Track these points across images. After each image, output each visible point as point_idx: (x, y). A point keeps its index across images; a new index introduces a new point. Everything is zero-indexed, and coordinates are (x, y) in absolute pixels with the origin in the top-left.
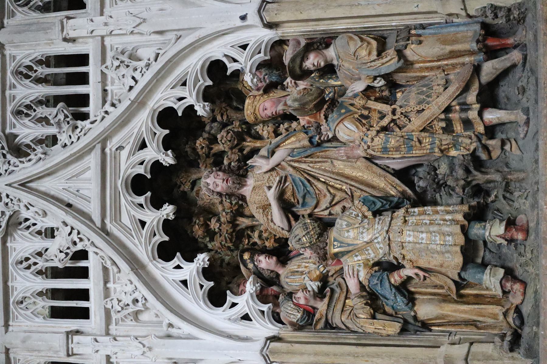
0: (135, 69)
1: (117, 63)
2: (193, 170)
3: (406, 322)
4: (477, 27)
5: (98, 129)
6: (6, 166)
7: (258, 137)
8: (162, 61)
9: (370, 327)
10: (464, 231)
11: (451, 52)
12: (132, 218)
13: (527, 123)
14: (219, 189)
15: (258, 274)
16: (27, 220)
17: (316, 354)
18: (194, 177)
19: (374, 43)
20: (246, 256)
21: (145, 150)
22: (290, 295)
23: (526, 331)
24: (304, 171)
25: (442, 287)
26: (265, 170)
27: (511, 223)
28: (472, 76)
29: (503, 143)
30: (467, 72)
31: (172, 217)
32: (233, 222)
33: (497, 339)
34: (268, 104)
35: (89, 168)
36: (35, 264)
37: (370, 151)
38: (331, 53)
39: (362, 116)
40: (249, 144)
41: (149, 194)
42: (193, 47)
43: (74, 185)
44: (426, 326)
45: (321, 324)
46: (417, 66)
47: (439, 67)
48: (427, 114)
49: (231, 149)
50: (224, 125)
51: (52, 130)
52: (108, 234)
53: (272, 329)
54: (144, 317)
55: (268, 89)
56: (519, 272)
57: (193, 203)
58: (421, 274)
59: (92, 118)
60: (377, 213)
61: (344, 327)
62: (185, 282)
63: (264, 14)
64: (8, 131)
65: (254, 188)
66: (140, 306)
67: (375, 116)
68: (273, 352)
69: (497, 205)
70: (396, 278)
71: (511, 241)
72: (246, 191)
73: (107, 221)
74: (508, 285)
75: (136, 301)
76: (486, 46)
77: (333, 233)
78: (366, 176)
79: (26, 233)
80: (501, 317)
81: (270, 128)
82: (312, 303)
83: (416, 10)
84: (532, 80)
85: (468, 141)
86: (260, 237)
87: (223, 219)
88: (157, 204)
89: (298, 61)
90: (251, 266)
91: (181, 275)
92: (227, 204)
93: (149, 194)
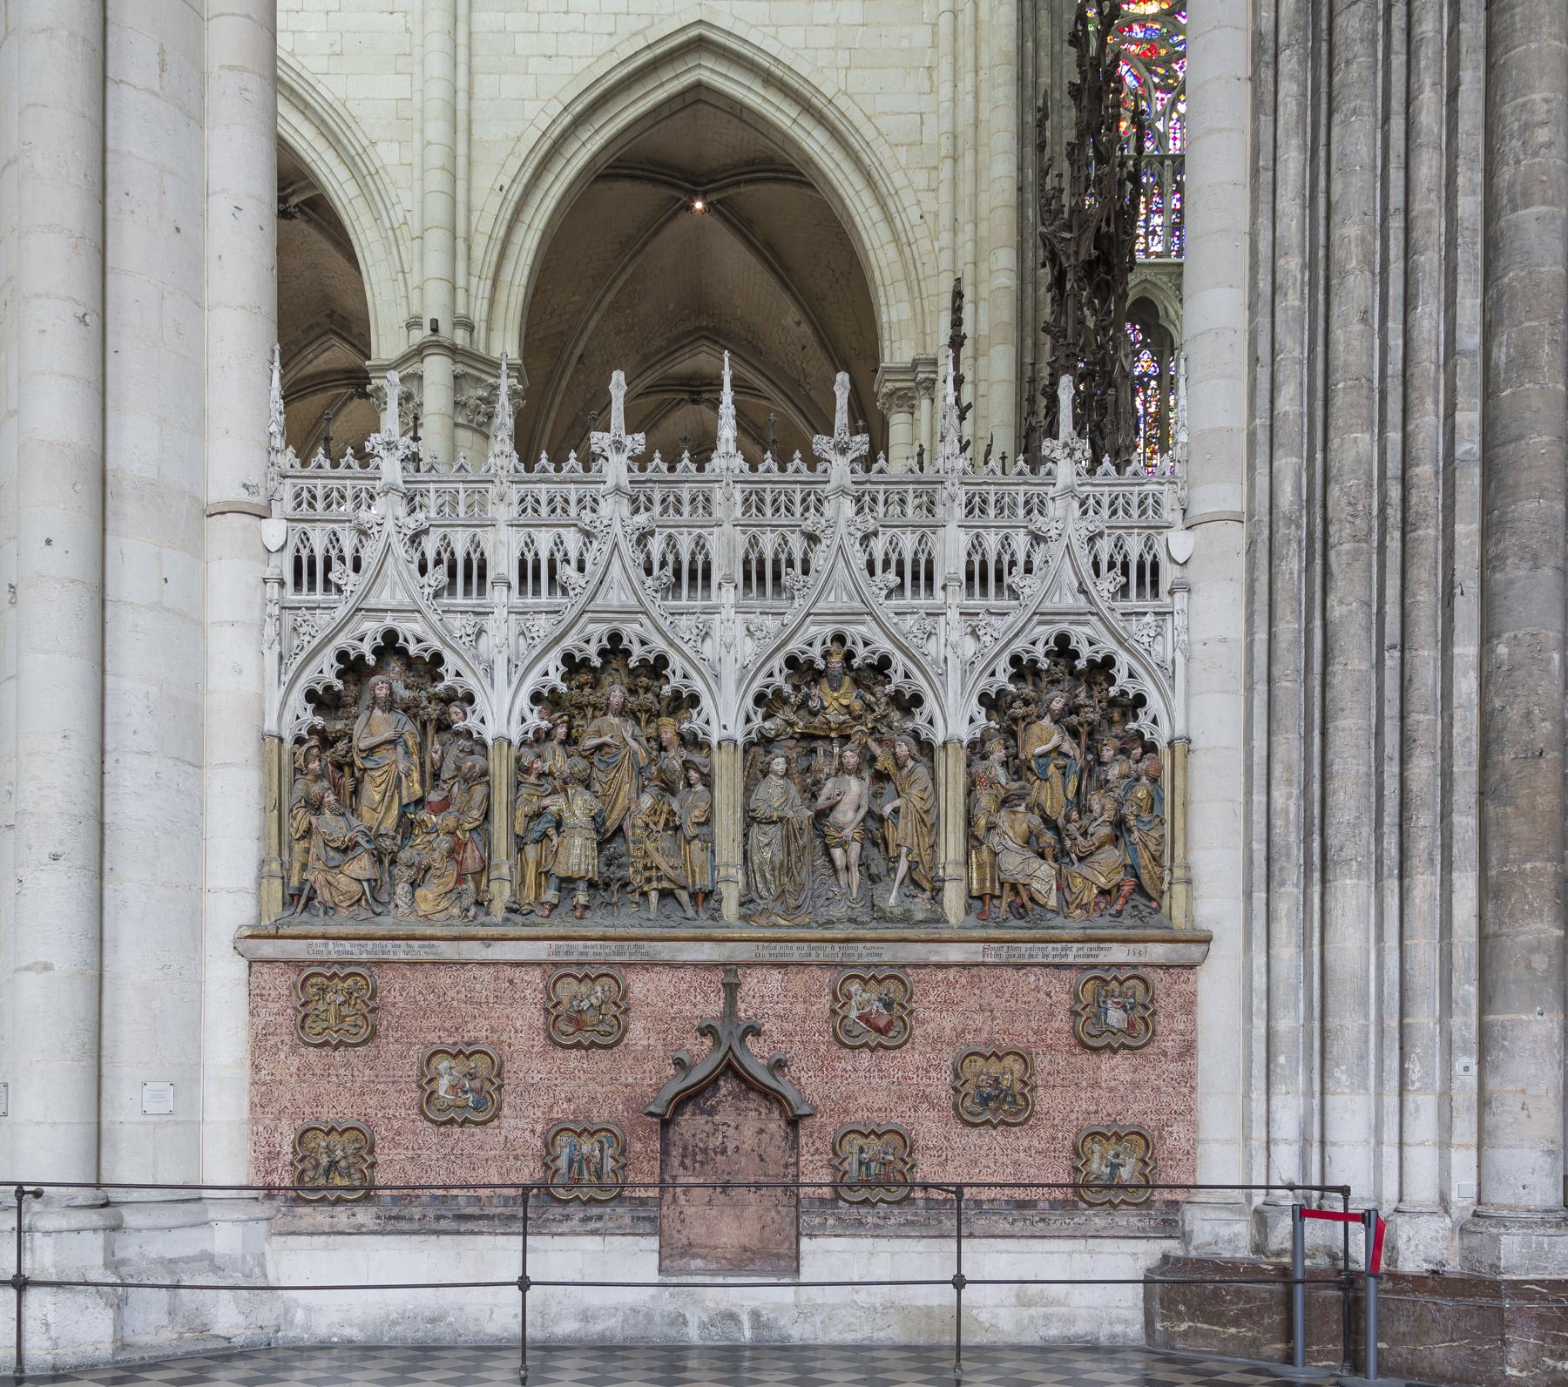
8: (700, 664)
9: (519, 813)
10: (582, 878)
23: (517, 918)
27: (586, 907)
30: (683, 883)
38: (700, 787)
43: (615, 586)
44: (521, 850)
48: (656, 855)
53: (516, 741)
55: (680, 736)
56: (555, 912)
60: (593, 818)
70: (551, 832)
77: (580, 789)
78: (618, 806)
88: (602, 653)
91: (552, 671)
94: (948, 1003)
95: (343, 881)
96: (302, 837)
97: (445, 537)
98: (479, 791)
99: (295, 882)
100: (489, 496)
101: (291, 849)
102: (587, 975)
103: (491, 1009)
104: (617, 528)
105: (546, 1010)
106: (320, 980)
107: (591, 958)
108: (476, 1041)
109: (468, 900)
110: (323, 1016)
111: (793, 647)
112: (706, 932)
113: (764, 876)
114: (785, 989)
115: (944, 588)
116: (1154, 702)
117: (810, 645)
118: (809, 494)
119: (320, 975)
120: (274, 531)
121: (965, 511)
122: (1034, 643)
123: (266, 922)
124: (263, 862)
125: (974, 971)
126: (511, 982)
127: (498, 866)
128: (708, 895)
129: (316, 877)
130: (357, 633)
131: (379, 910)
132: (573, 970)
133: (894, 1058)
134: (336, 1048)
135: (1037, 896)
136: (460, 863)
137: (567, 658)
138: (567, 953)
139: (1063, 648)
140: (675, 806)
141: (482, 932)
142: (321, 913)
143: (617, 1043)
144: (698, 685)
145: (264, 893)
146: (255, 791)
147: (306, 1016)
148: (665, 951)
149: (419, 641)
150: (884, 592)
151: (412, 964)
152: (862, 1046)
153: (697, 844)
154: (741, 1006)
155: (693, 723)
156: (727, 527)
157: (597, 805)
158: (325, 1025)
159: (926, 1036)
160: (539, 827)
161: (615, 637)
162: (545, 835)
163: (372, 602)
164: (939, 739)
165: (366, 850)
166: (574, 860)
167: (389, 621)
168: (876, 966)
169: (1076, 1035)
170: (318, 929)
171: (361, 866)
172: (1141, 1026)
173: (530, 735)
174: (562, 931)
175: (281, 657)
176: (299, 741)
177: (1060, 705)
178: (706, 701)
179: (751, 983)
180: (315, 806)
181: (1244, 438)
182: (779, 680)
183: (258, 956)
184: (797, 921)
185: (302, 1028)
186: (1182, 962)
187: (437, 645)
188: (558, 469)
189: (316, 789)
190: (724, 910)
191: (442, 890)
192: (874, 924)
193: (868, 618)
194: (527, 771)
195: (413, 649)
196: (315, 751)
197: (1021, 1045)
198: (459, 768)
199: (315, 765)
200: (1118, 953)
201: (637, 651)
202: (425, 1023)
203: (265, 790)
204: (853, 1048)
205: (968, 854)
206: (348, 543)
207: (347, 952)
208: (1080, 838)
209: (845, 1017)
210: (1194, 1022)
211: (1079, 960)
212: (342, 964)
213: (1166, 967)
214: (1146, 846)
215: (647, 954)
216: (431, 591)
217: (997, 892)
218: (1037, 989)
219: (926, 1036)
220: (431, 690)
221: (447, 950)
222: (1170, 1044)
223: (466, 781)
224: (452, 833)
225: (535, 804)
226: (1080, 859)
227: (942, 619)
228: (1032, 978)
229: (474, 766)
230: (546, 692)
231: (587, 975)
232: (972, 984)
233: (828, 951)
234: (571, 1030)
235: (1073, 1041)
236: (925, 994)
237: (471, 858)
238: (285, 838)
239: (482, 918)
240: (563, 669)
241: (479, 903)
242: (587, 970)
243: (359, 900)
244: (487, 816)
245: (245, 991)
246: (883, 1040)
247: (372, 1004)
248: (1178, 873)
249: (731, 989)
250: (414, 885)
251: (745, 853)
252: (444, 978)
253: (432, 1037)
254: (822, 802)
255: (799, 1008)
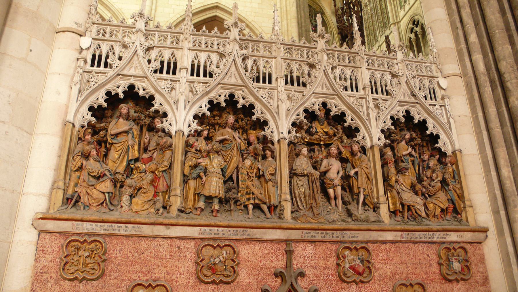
0: (267, 98)
1: (270, 93)
2: (233, 113)
3: (188, 176)
4: (277, 204)
5: (250, 85)
6: (240, 55)
7: (243, 134)
8: (270, 107)
9: (187, 165)
10: (216, 197)
11: (270, 196)
12: (222, 93)
13: (249, 218)
14: (229, 121)
15: (202, 131)
16: (222, 60)
17: (179, 147)
18: (231, 113)
19: (273, 172)
20: (208, 127)
21: (242, 99)
22: (197, 140)
24: (234, 147)
25: (198, 188)
26: (234, 136)
27: (218, 211)
28: (263, 202)
29: (242, 210)
30: (264, 200)
31: (221, 105)
32: (218, 124)
33: (182, 205)
34: (253, 138)
35: (237, 81)
36: (208, 61)
37: (241, 169)
39: (252, 167)
40: (241, 131)
41: (229, 99)
42: (274, 118)
45: (188, 150)
46: (266, 185)
47: (265, 191)
48: (252, 187)
49: (240, 125)
50: (246, 123)
51: (249, 70)
52: (217, 85)
53: (186, 134)
54: (191, 94)
55: (258, 138)
56: (203, 213)
57: (223, 112)
58: (203, 182)
59: (253, 84)
60: (222, 169)
61: (187, 157)
62: (201, 107)
63: (283, 139)
64: (250, 57)
65: (228, 131)
66: (195, 93)
67: (251, 171)
68: (179, 134)
69: (222, 207)
70: (202, 174)
71: (212, 211)
72: (228, 129)
73: (221, 85)
74: (199, 210)
75: (197, 92)
76: (271, 206)
77: (216, 155)
78: (231, 167)
79: (218, 59)
80: (189, 207)
81: (246, 138)
82: (195, 147)
83: (283, 185)
84: (261, 220)
85: (243, 199)
86: (213, 132)
87: (219, 121)
88: (225, 101)
89: (269, 149)
90: (205, 128)
91: (204, 106)
92: (223, 122)
93: (229, 99)
94: (388, 260)
95: (95, 193)
96: (77, 170)
97: (160, 51)
98: (168, 154)
99: (70, 192)
100: (181, 39)
101: (70, 177)
102: (218, 245)
103: (167, 262)
104: (235, 53)
105: (197, 264)
106: (76, 243)
107: (220, 236)
108: (159, 279)
109: (159, 205)
110: (76, 263)
111: (307, 105)
112: (275, 225)
113: (301, 200)
114: (315, 254)
115: (363, 89)
116: (443, 137)
117: (314, 105)
118: (309, 52)
119: (77, 240)
120: (86, 42)
121: (367, 64)
122: (398, 112)
123: (52, 211)
124: (54, 182)
125: (397, 245)
126: (179, 248)
127: (175, 189)
128: (276, 207)
129: (82, 190)
130: (117, 84)
131: (112, 208)
132: (211, 243)
133: (367, 287)
134: (81, 281)
135: (418, 211)
136: (156, 187)
137: (210, 102)
138: (209, 234)
139: (408, 116)
140: (260, 167)
141: (166, 221)
142: (82, 208)
143: (232, 281)
144: (268, 117)
145: (53, 197)
146: (57, 148)
147: (66, 263)
148: (258, 234)
149: (144, 90)
150: (342, 87)
151: (127, 236)
152: (352, 282)
153: (270, 184)
154: (295, 262)
155: (267, 132)
156: (279, 59)
157: (224, 164)
158: (76, 268)
159: (380, 276)
160: (196, 172)
161: (232, 96)
162: (199, 176)
163: (125, 72)
164: (368, 145)
165: (109, 178)
166: (213, 188)
167: (132, 81)
168: (356, 242)
169: (441, 274)
170: (78, 216)
171: (106, 186)
172: (466, 270)
173: (192, 132)
174: (207, 223)
175: (80, 91)
176: (83, 127)
177: (409, 137)
178: (271, 123)
179: (299, 250)
180: (86, 156)
181: (455, 52)
182: (302, 117)
183: (44, 229)
184: (319, 220)
185: (63, 269)
186: (477, 240)
187: (152, 91)
188: (210, 32)
189: (88, 148)
190: (285, 214)
191: (146, 199)
192: (353, 222)
193: (336, 97)
194: (192, 146)
195: (141, 93)
196: (90, 130)
197: (419, 281)
198: (158, 144)
199: (88, 137)
200: (453, 237)
201: (241, 102)
202: (132, 269)
203: (61, 148)
204: (348, 283)
205: (386, 194)
206: (118, 49)
207: (93, 229)
208: (429, 187)
209: (344, 267)
210: (485, 267)
211: (439, 240)
212: (89, 235)
213: (471, 243)
214: (455, 191)
215: (249, 235)
216: (153, 69)
217: (401, 210)
218: (423, 253)
219: (380, 276)
220: (147, 113)
221: (147, 230)
222: (479, 278)
223: (161, 149)
224: (153, 172)
225: (194, 161)
226: (430, 196)
227: (364, 100)
228: (421, 248)
229: (166, 142)
230: (200, 115)
231: (218, 245)
232: (396, 250)
233: (335, 235)
234: (209, 273)
235: (441, 277)
236: (377, 256)
237: (162, 185)
238: (69, 171)
239: (165, 214)
240: (208, 106)
241: (164, 207)
242: (218, 242)
243: (102, 203)
244: (170, 166)
245: (34, 248)
246: (361, 278)
247: (104, 257)
248: (467, 203)
249: (289, 253)
250: (132, 196)
251: (290, 189)
252: (143, 244)
253: (135, 276)
254: (322, 169)
255: (322, 263)
